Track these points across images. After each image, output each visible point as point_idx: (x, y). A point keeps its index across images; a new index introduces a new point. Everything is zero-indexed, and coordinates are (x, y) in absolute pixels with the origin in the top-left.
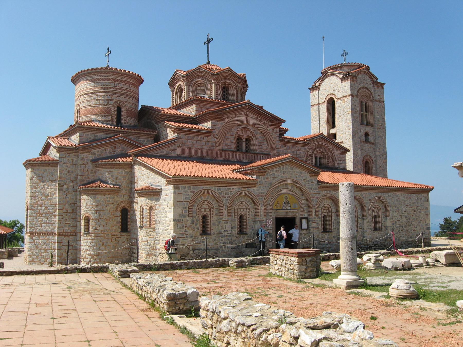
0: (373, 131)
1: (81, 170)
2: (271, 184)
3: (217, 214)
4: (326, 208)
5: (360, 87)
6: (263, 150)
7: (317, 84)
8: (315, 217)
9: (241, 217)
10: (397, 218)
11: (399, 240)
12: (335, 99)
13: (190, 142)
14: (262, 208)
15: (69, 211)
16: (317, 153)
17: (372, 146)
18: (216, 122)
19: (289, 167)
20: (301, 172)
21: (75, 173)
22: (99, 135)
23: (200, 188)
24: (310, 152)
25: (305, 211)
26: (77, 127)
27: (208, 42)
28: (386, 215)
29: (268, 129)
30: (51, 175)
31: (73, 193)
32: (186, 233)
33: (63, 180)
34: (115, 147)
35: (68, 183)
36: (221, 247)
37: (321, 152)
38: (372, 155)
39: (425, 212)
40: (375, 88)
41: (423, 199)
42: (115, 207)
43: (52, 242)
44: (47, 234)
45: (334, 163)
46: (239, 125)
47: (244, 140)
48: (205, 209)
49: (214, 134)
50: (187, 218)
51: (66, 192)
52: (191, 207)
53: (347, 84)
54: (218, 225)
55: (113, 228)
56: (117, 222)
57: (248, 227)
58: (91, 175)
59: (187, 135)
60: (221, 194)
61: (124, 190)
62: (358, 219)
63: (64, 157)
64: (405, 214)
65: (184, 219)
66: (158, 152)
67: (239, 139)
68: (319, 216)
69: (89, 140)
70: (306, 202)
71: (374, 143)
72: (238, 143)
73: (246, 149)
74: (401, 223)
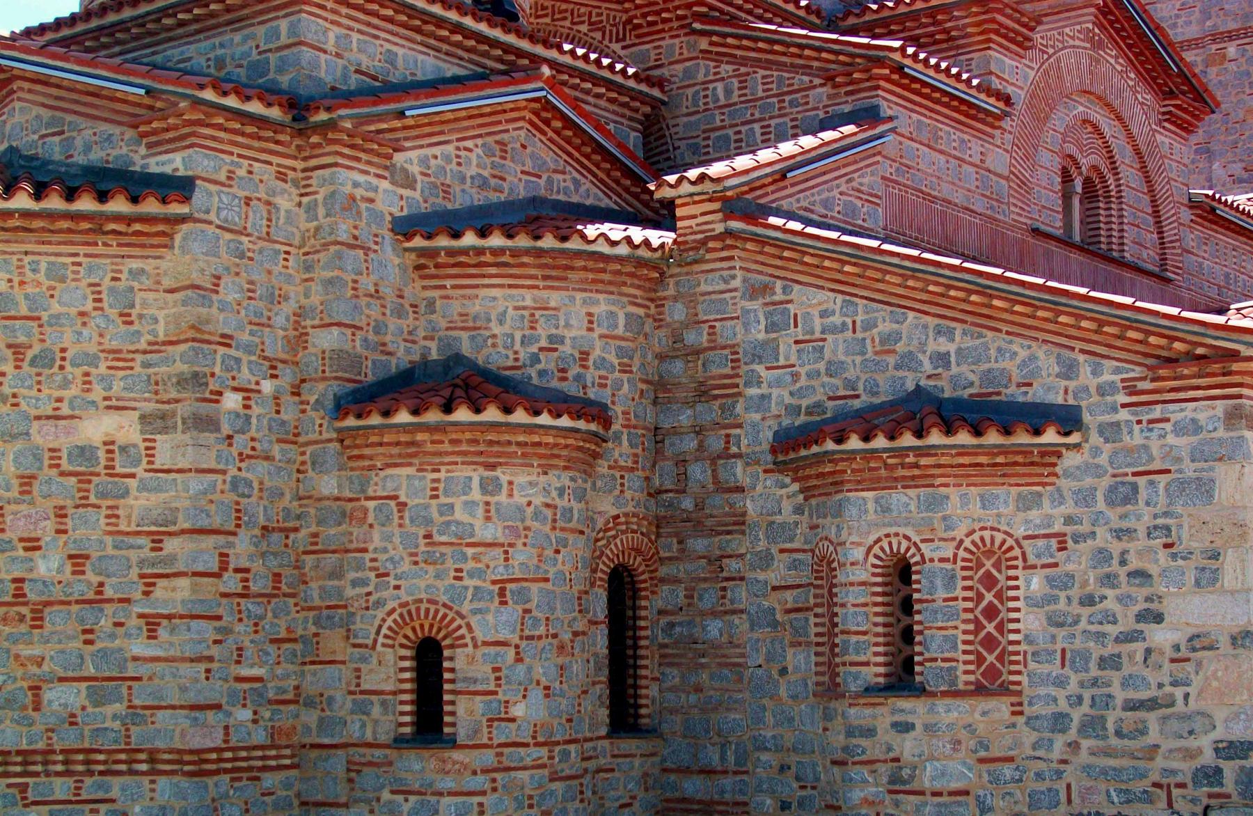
15: (254, 588)
18: (1006, 59)
21: (289, 308)
22: (400, 51)
30: (113, 313)
31: (276, 450)
33: (222, 350)
35: (245, 376)
59: (914, 116)
61: (625, 437)
63: (222, 177)
67: (1066, 178)
69: (354, 81)
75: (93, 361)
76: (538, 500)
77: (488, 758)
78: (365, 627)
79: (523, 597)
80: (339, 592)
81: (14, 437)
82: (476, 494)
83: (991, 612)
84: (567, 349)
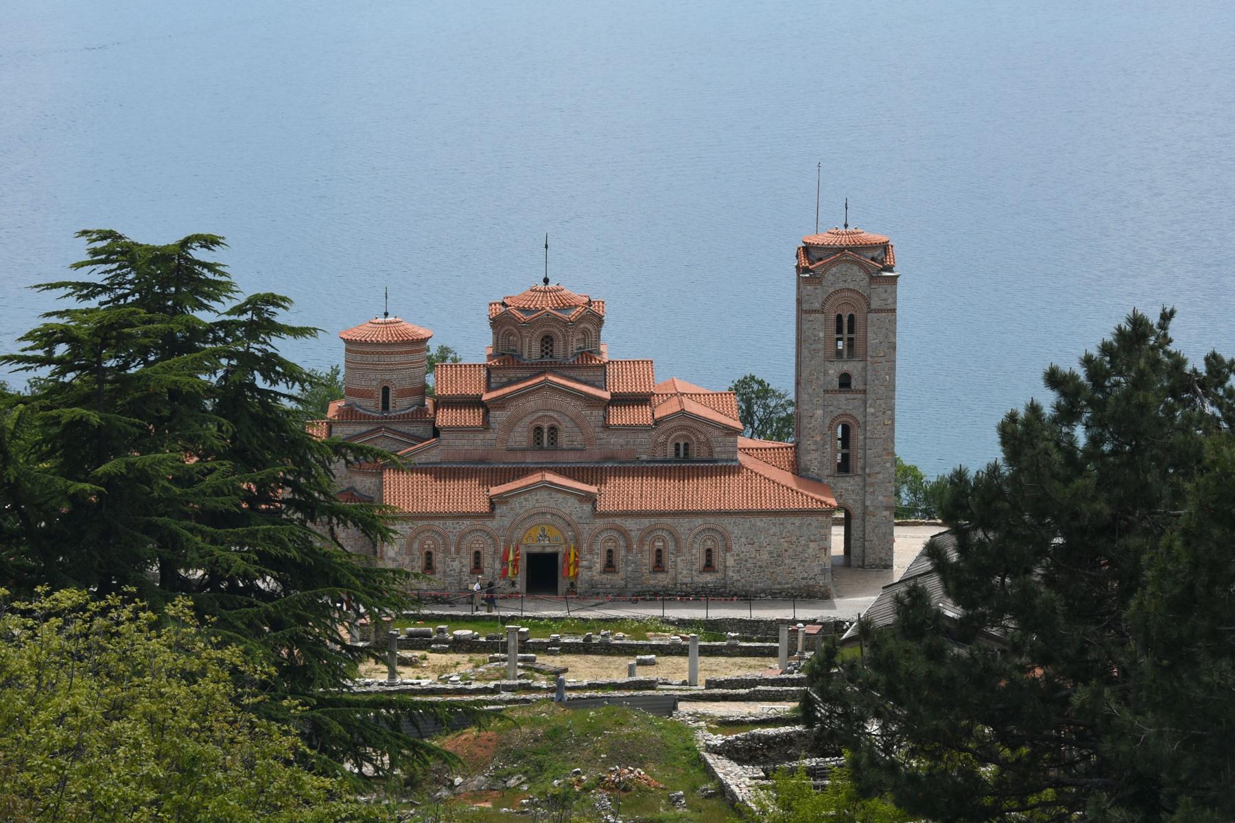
0: (865, 369)
2: (518, 515)
5: (831, 290)
6: (575, 443)
9: (477, 554)
17: (859, 396)
23: (420, 523)
24: (662, 439)
28: (728, 549)
39: (819, 545)
41: (815, 524)
45: (711, 453)
47: (546, 430)
48: (429, 545)
52: (410, 545)
57: (486, 565)
58: (344, 481)
64: (768, 549)
66: (416, 460)
67: (538, 430)
74: (759, 561)
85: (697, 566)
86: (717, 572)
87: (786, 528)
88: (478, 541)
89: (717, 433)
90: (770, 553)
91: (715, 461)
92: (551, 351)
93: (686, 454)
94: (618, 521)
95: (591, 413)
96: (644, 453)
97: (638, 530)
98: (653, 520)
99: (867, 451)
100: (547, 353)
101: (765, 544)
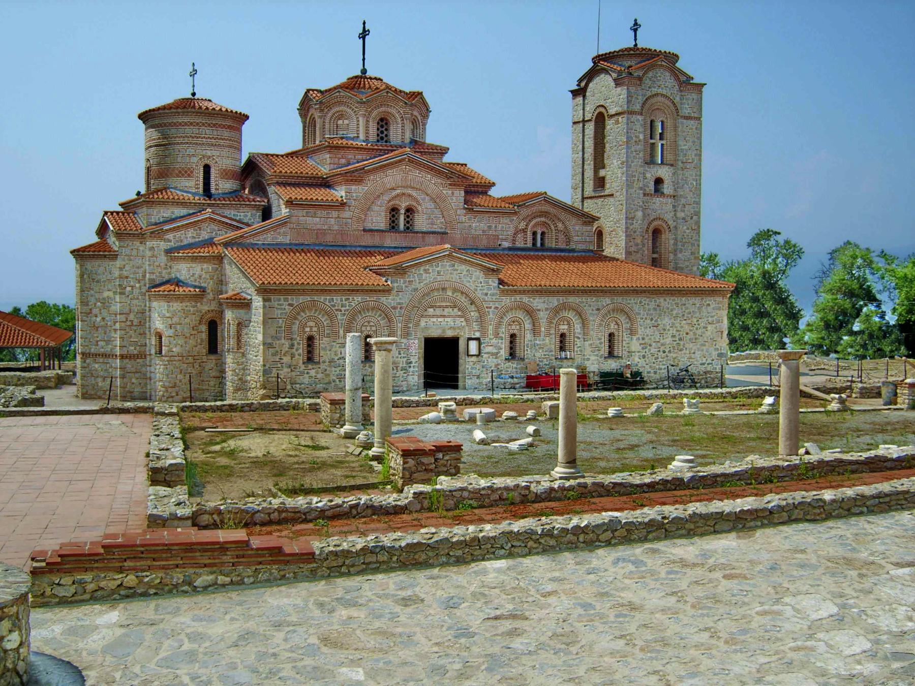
0: (674, 174)
1: (149, 265)
2: (416, 290)
3: (327, 334)
4: (516, 323)
5: (649, 94)
7: (583, 84)
8: (492, 337)
10: (652, 337)
11: (655, 373)
12: (606, 115)
13: (309, 220)
14: (399, 325)
16: (534, 226)
17: (670, 200)
18: (353, 187)
19: (448, 264)
20: (468, 270)
23: (301, 299)
24: (522, 225)
25: (476, 328)
26: (144, 201)
27: (364, 34)
28: (632, 332)
29: (444, 192)
31: (140, 297)
32: (282, 361)
34: (200, 229)
35: (132, 283)
36: (334, 381)
37: (544, 224)
38: (669, 217)
39: (716, 328)
40: (683, 94)
42: (198, 319)
43: (112, 367)
44: (105, 355)
45: (568, 240)
46: (393, 189)
47: (403, 211)
48: (311, 327)
49: (349, 206)
50: (283, 341)
51: (130, 296)
53: (622, 92)
54: (330, 350)
55: (197, 349)
56: (202, 340)
58: (164, 272)
60: (334, 306)
62: (576, 339)
65: (278, 342)
67: (394, 211)
68: (501, 335)
69: (161, 220)
70: (477, 314)
71: (674, 196)
72: (393, 216)
73: (407, 225)
74: (662, 345)
75: (104, 281)
76: (180, 309)
77: (166, 359)
78: (152, 330)
79: (175, 328)
80: (149, 325)
81: (92, 296)
82: (166, 308)
83: (241, 335)
84: (196, 276)
85: (602, 352)
86: (621, 357)
87: (687, 308)
88: (369, 322)
89: (574, 221)
90: (673, 336)
91: (573, 251)
92: (386, 136)
93: (542, 244)
94: (525, 299)
95: (453, 193)
96: (505, 240)
97: (547, 309)
98: (562, 299)
99: (680, 255)
100: (382, 138)
101: (668, 327)
